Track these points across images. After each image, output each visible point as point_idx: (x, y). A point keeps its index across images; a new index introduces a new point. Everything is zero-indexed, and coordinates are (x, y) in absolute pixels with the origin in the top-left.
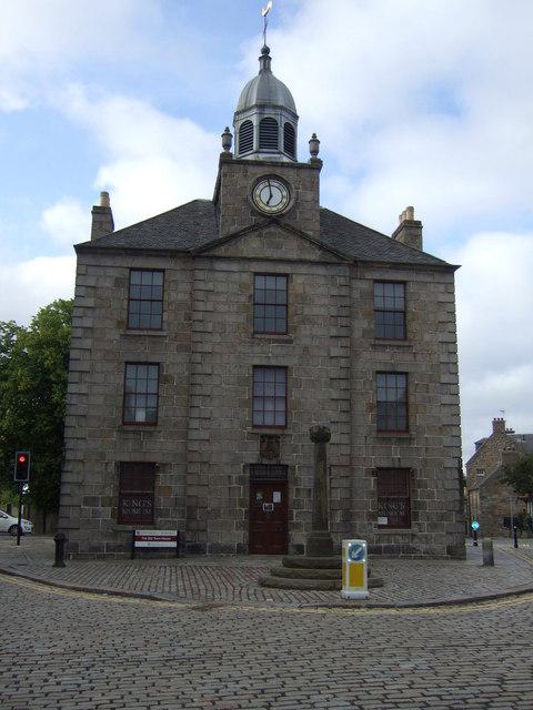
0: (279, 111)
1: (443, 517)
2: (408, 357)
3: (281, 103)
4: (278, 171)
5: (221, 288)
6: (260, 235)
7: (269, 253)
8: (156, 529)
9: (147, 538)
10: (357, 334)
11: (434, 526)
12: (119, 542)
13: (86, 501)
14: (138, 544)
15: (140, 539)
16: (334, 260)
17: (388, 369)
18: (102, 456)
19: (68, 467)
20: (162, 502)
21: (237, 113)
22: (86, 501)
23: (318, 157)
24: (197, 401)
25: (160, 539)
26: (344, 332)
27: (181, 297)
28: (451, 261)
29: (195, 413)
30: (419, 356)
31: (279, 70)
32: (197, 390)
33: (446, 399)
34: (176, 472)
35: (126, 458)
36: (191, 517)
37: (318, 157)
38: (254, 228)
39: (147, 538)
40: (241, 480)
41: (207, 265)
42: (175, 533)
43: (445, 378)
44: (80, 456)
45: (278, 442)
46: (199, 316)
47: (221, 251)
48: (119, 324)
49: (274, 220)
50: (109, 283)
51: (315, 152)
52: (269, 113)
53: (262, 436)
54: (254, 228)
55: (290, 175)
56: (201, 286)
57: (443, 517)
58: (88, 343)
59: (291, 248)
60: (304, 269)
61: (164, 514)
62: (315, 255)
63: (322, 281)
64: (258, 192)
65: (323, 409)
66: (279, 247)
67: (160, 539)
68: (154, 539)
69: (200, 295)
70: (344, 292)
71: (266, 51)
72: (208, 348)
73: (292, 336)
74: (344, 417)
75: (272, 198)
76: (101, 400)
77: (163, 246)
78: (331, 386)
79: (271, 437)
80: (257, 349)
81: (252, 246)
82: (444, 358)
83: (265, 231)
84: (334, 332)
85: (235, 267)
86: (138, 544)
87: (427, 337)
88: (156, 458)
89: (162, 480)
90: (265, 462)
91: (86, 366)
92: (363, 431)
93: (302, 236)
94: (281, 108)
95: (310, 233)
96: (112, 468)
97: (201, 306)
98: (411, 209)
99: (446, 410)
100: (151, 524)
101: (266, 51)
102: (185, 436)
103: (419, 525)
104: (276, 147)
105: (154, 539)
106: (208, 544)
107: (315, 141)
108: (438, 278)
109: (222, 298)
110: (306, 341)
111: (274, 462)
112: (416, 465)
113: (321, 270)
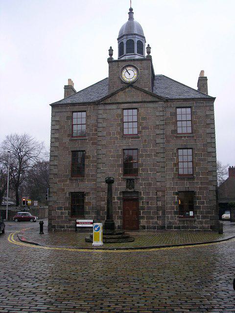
0: (134, 36)
3: (136, 33)
4: (132, 63)
7: (129, 100)
12: (71, 225)
14: (78, 225)
15: (78, 223)
16: (157, 100)
18: (63, 190)
20: (87, 208)
21: (118, 39)
23: (150, 54)
24: (100, 166)
25: (86, 223)
27: (92, 122)
28: (214, 97)
29: (99, 171)
31: (137, 18)
32: (100, 161)
33: (210, 159)
34: (91, 196)
37: (150, 54)
38: (122, 89)
43: (210, 150)
45: (134, 182)
46: (100, 129)
47: (109, 101)
49: (130, 85)
51: (149, 52)
52: (130, 37)
53: (127, 180)
54: (122, 89)
55: (138, 65)
57: (208, 212)
61: (88, 213)
64: (124, 74)
67: (86, 223)
68: (84, 223)
69: (100, 121)
71: (131, 10)
75: (130, 75)
77: (86, 101)
79: (130, 180)
80: (124, 142)
82: (209, 141)
83: (127, 90)
85: (114, 107)
86: (78, 225)
88: (86, 191)
94: (135, 34)
95: (147, 89)
96: (67, 195)
97: (100, 125)
98: (202, 72)
100: (84, 218)
101: (131, 10)
102: (95, 180)
104: (133, 52)
105: (84, 223)
107: (149, 48)
108: (205, 103)
111: (132, 190)
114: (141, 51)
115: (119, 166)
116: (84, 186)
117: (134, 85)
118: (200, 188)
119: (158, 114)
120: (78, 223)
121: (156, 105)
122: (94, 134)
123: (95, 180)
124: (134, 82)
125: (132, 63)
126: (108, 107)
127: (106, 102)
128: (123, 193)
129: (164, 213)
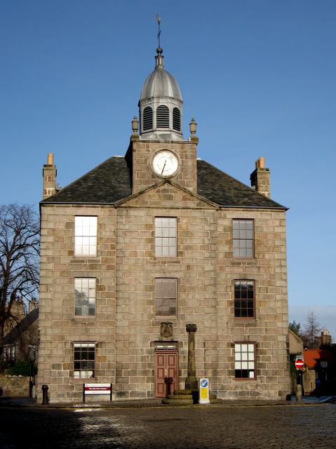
1: (276, 373)
5: (134, 228)
6: (158, 191)
8: (97, 383)
9: (92, 389)
11: (270, 379)
13: (54, 367)
14: (86, 392)
15: (88, 389)
17: (242, 277)
18: (62, 338)
19: (42, 346)
22: (54, 367)
24: (120, 302)
25: (100, 389)
26: (213, 255)
27: (108, 233)
29: (119, 310)
30: (262, 270)
32: (120, 295)
34: (110, 347)
36: (118, 373)
39: (92, 389)
42: (109, 385)
44: (49, 338)
46: (119, 247)
49: (167, 180)
56: (121, 227)
63: (198, 221)
65: (200, 305)
66: (170, 198)
67: (100, 389)
68: (96, 389)
70: (212, 228)
72: (126, 268)
74: (212, 310)
76: (60, 303)
78: (205, 290)
79: (167, 324)
81: (152, 196)
84: (207, 255)
87: (267, 256)
90: (164, 339)
91: (50, 281)
92: (225, 319)
93: (185, 190)
99: (279, 304)
102: (113, 324)
103: (261, 377)
105: (96, 389)
106: (130, 391)
109: (134, 235)
110: (188, 262)
111: (169, 339)
113: (197, 214)
114: (177, 126)
118: (265, 338)
119: (207, 228)
120: (88, 389)
122: (110, 253)
123: (113, 324)
124: (171, 177)
125: (169, 146)
126: (133, 213)
127: (131, 206)
129: (215, 373)
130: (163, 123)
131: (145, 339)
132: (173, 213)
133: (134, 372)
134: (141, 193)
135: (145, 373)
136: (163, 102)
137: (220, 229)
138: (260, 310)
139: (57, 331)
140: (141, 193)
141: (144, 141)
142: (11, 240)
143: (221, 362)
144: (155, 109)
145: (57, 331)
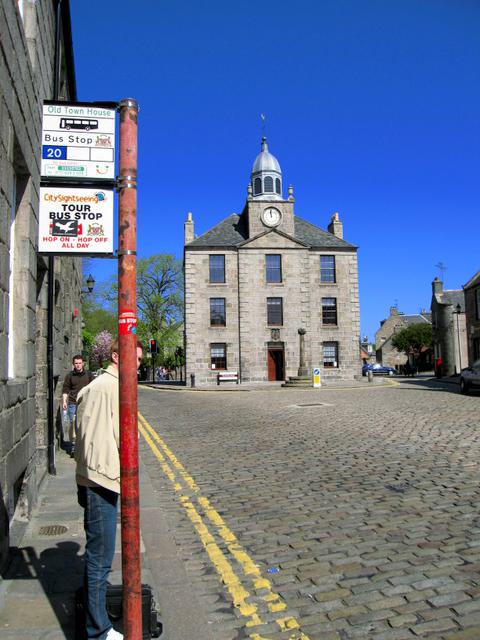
1: (352, 363)
2: (336, 291)
4: (274, 205)
10: (312, 281)
13: (197, 361)
14: (221, 378)
18: (202, 341)
25: (230, 376)
35: (213, 342)
38: (265, 233)
40: (263, 350)
41: (244, 251)
48: (206, 281)
49: (274, 229)
50: (200, 262)
57: (352, 363)
58: (193, 290)
59: (282, 242)
60: (288, 251)
62: (293, 245)
66: (276, 241)
68: (227, 376)
70: (306, 261)
73: (284, 283)
76: (199, 316)
81: (263, 241)
85: (256, 251)
86: (221, 378)
87: (345, 281)
89: (229, 350)
96: (208, 346)
105: (227, 376)
110: (289, 286)
112: (340, 340)
115: (263, 315)
116: (227, 335)
117: (278, 228)
121: (301, 251)
125: (274, 205)
126: (249, 251)
128: (269, 343)
130: (269, 189)
131: (261, 340)
132: (278, 252)
133: (254, 364)
134: (256, 238)
135: (261, 364)
136: (268, 174)
137: (312, 262)
138: (340, 319)
139: (199, 336)
140: (256, 238)
141: (256, 201)
142: (160, 277)
143: (314, 356)
144: (263, 178)
145: (199, 336)
